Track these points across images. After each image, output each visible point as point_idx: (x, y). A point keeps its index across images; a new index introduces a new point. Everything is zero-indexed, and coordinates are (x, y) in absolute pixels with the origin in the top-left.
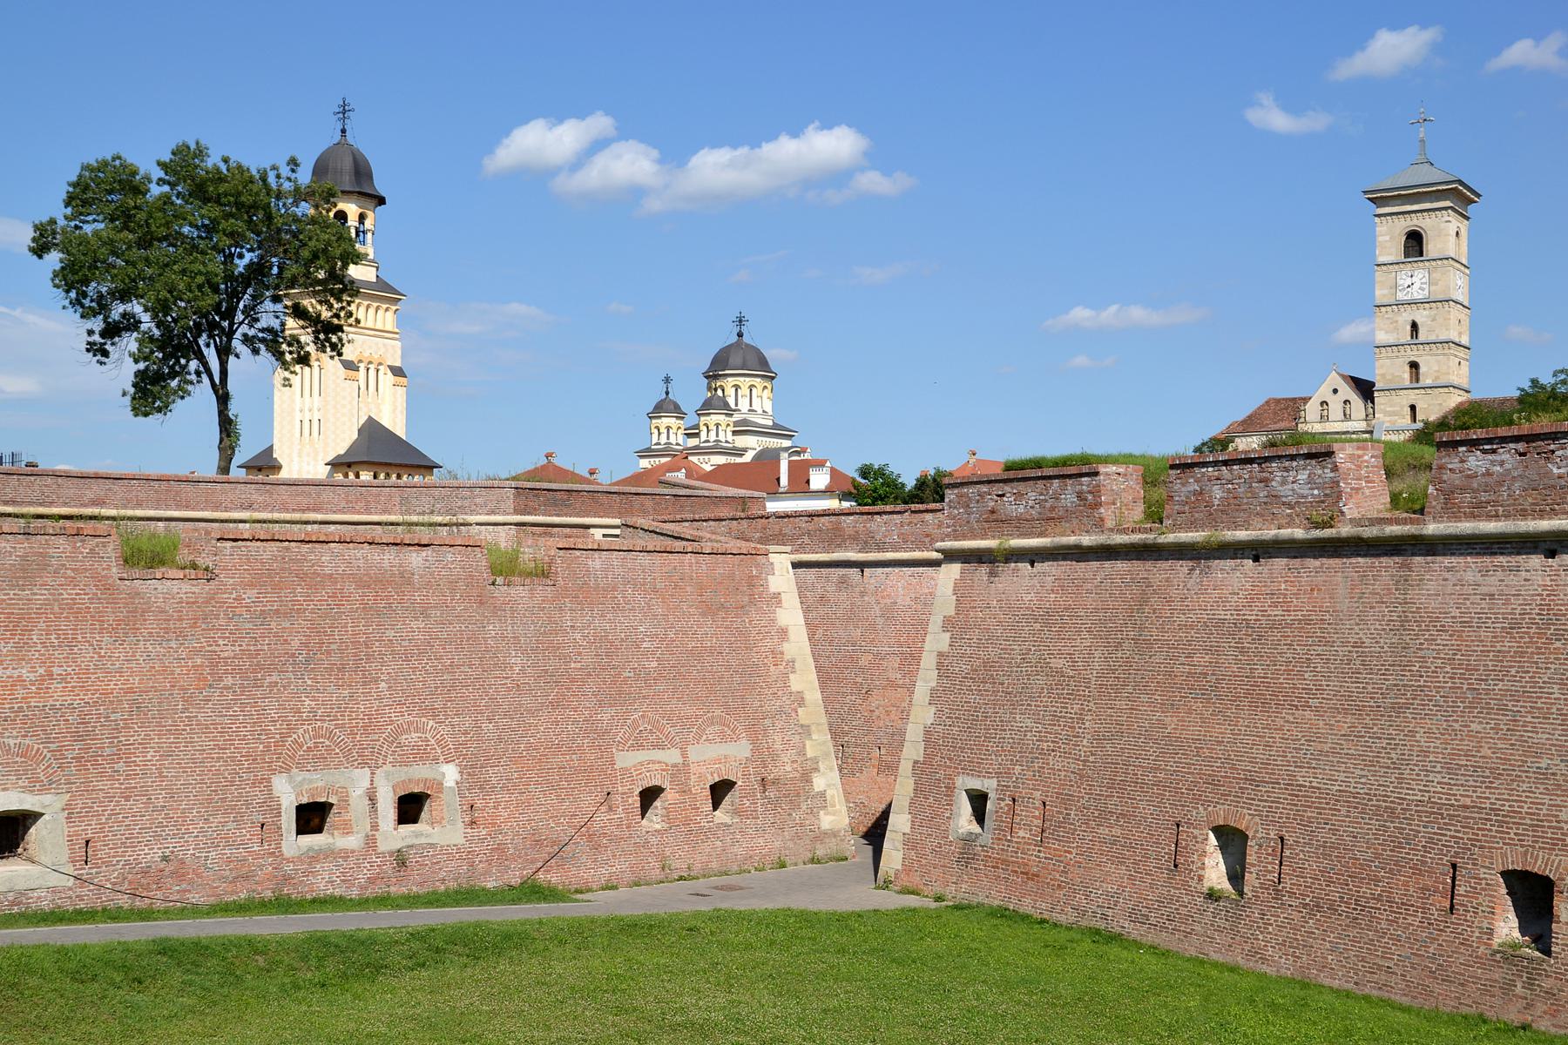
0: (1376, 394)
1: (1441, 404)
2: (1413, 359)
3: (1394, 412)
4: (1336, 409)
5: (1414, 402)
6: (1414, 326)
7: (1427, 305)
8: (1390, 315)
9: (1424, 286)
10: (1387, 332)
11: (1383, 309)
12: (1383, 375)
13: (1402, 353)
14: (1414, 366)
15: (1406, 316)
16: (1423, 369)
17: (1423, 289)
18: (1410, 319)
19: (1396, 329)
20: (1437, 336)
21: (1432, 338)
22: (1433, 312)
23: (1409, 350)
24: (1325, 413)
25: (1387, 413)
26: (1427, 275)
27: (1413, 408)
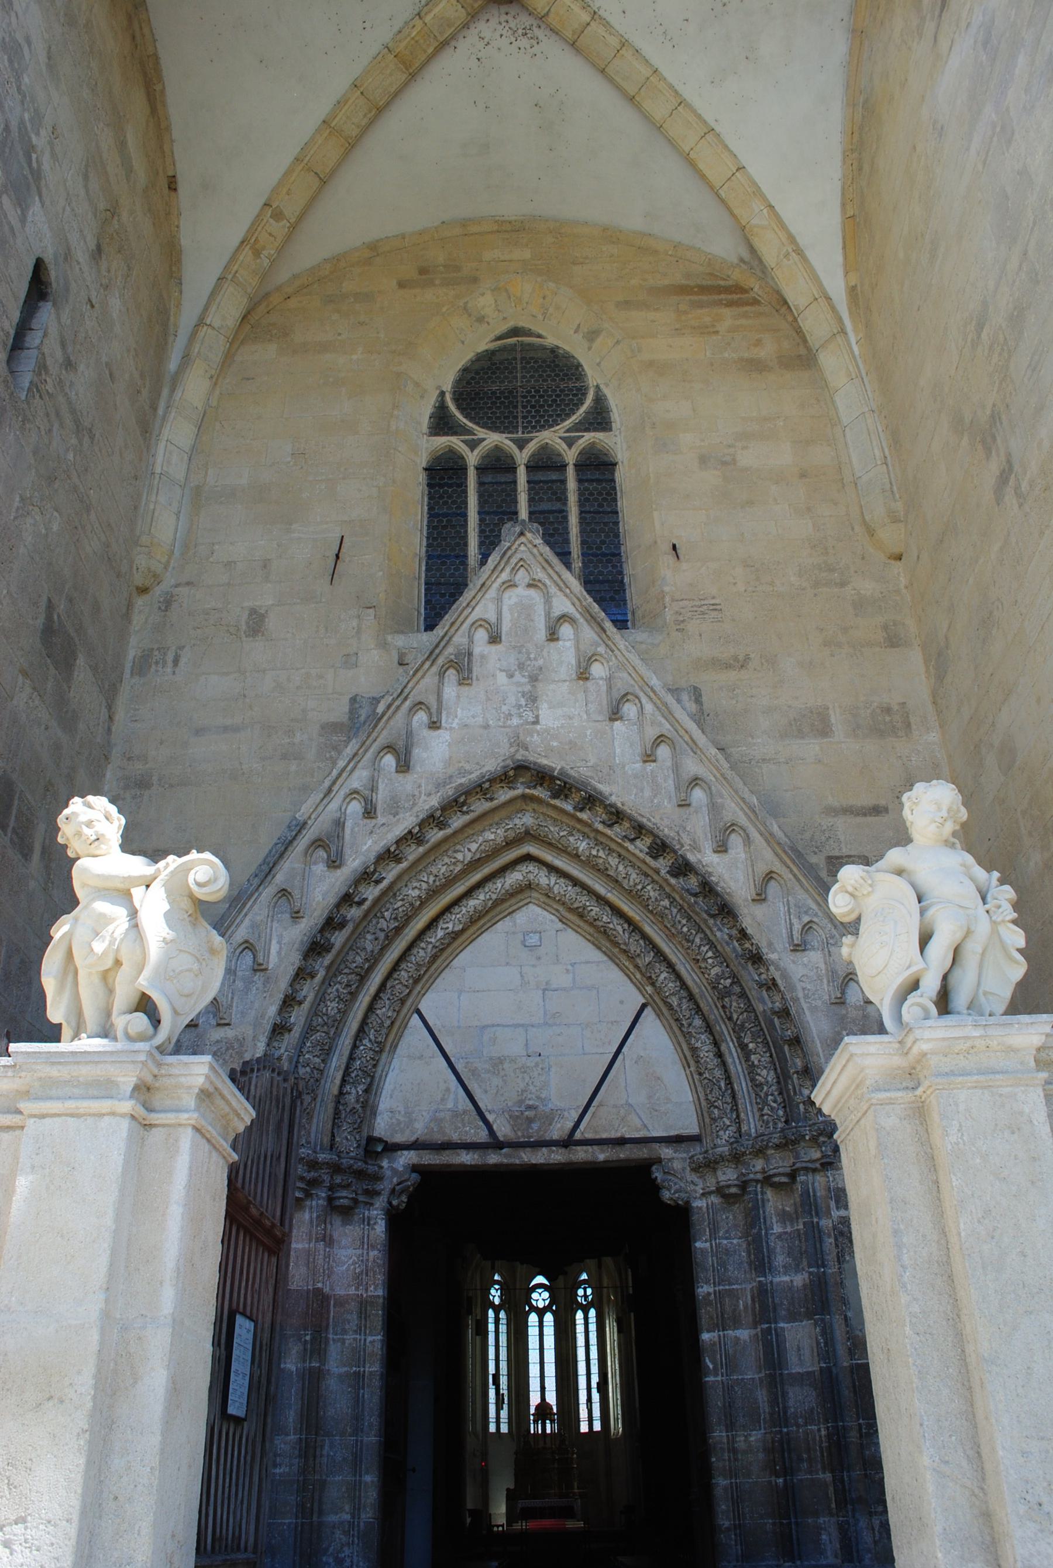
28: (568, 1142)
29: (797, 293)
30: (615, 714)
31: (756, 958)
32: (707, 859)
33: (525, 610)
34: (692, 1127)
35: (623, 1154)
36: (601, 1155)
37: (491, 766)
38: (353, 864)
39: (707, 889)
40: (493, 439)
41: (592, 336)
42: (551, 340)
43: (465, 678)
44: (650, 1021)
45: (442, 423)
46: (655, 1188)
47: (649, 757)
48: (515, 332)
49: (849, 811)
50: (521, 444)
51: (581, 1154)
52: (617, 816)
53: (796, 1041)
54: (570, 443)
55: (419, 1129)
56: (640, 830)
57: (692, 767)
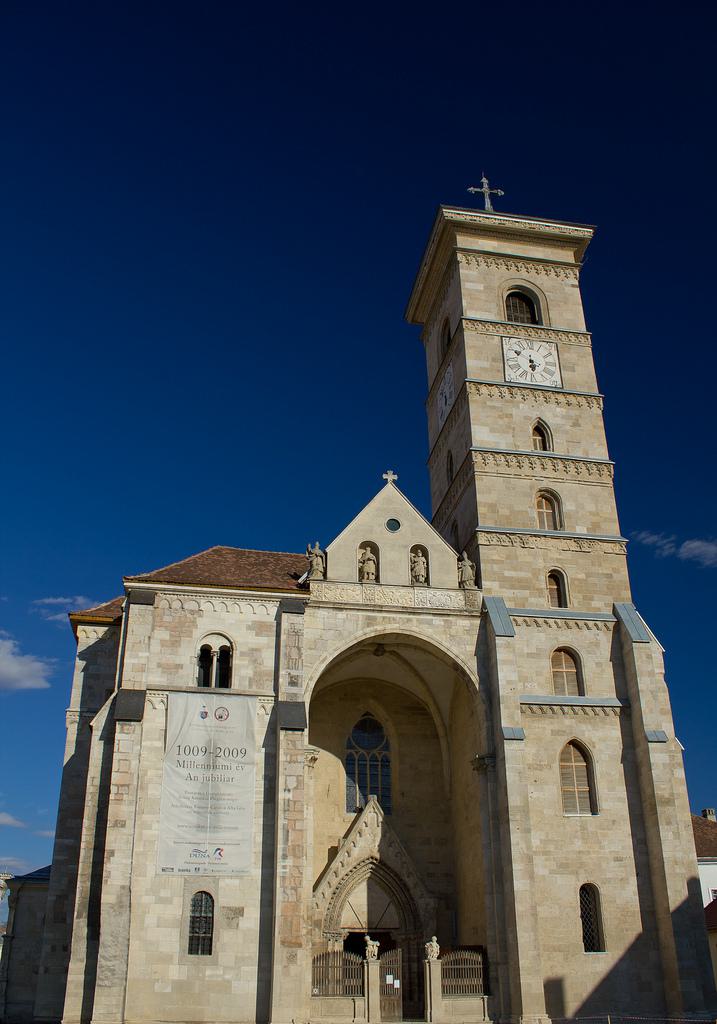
0: (482, 539)
1: (609, 576)
2: (546, 484)
3: (520, 580)
4: (395, 559)
5: (557, 566)
6: (540, 430)
7: (561, 398)
8: (497, 403)
9: (552, 369)
10: (492, 430)
11: (484, 389)
12: (493, 507)
13: (526, 469)
14: (550, 498)
15: (527, 411)
16: (568, 506)
17: (552, 374)
18: (535, 415)
19: (510, 429)
20: (587, 454)
21: (578, 454)
22: (574, 412)
23: (538, 467)
24: (370, 567)
25: (506, 582)
26: (555, 353)
27: (556, 577)
28: (376, 928)
29: (437, 721)
30: (390, 846)
31: (412, 899)
32: (407, 880)
33: (373, 818)
34: (397, 926)
35: (385, 931)
36: (382, 931)
37: (366, 857)
38: (340, 877)
39: (405, 885)
40: (362, 751)
41: (387, 720)
42: (376, 718)
43: (360, 836)
44: (392, 907)
45: (350, 747)
46: (390, 937)
47: (396, 856)
48: (367, 714)
49: (432, 863)
50: (368, 754)
51: (378, 931)
52: (389, 868)
53: (418, 915)
54: (380, 754)
55: (349, 925)
56: (392, 871)
57: (404, 859)
